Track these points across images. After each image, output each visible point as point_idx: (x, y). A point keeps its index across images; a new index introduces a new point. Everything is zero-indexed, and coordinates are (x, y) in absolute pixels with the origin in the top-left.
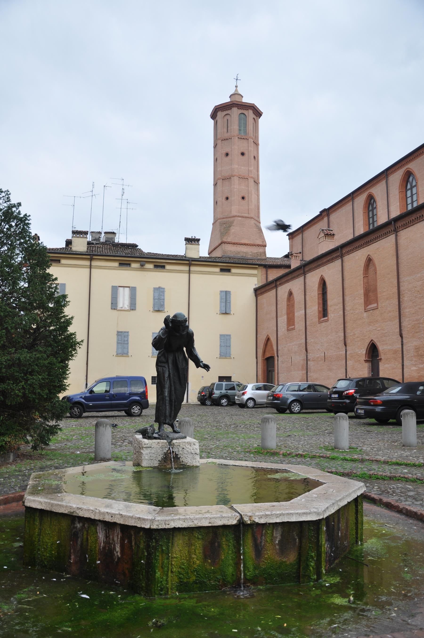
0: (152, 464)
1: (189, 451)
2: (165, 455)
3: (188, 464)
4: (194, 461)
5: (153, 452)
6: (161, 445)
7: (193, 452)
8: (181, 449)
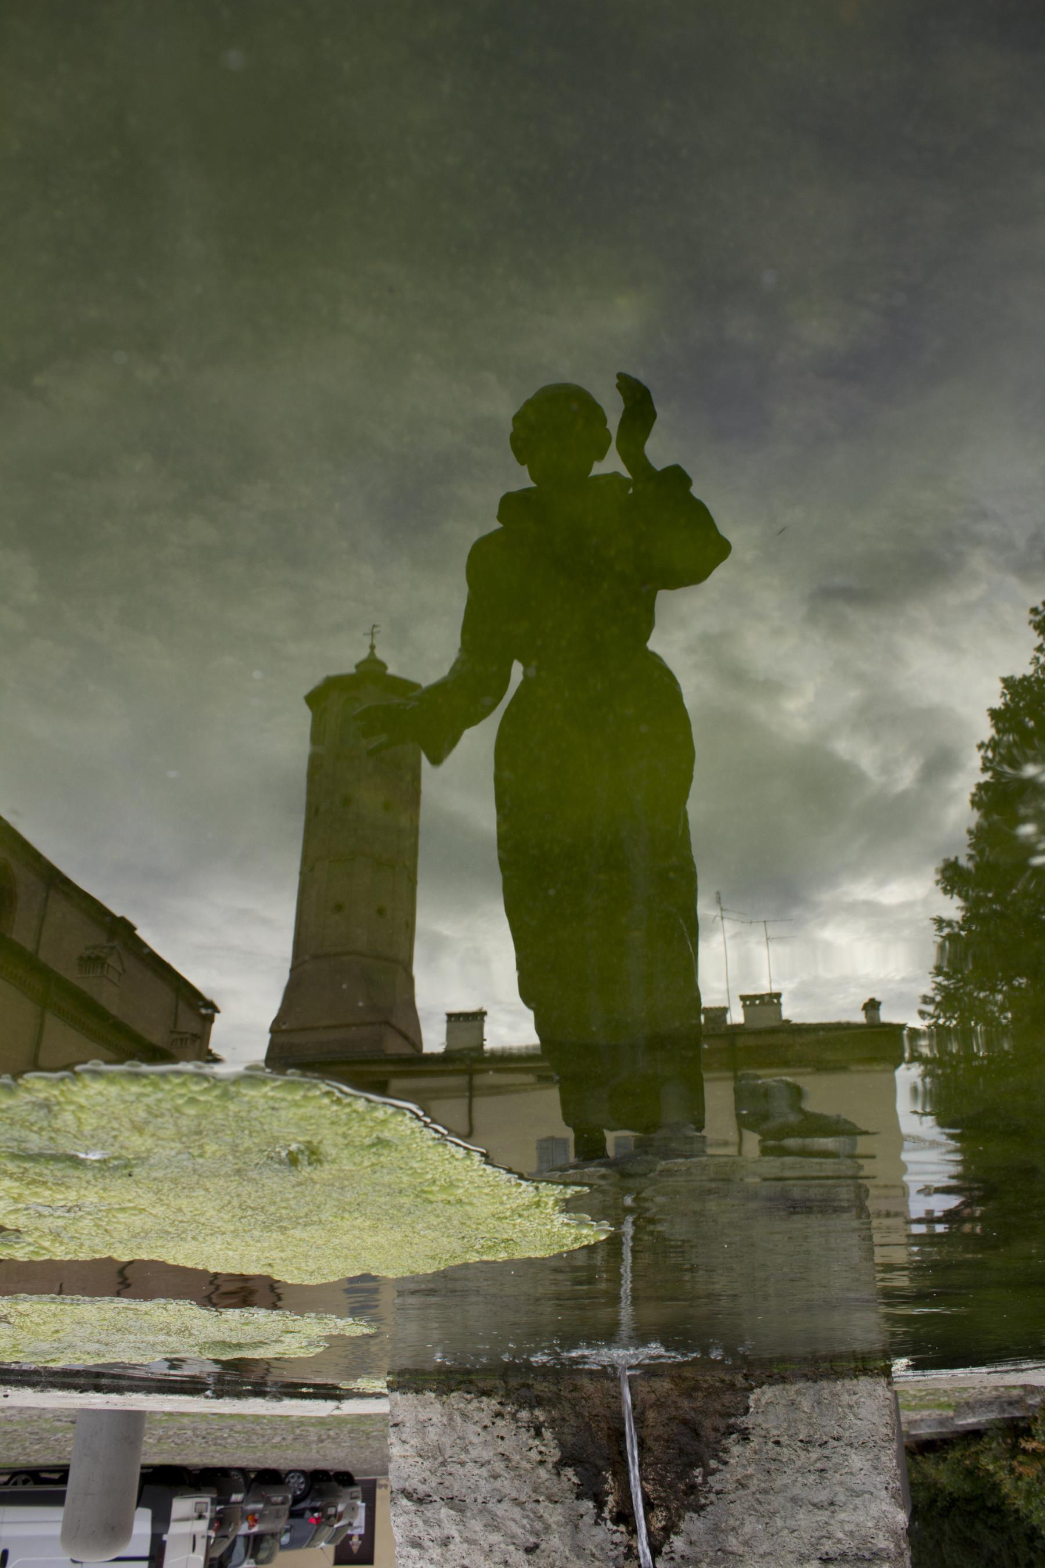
0: (806, 1404)
1: (476, 1525)
2: (692, 1488)
3: (491, 1404)
4: (432, 1435)
5: (804, 1519)
7: (445, 1512)
8: (556, 1542)
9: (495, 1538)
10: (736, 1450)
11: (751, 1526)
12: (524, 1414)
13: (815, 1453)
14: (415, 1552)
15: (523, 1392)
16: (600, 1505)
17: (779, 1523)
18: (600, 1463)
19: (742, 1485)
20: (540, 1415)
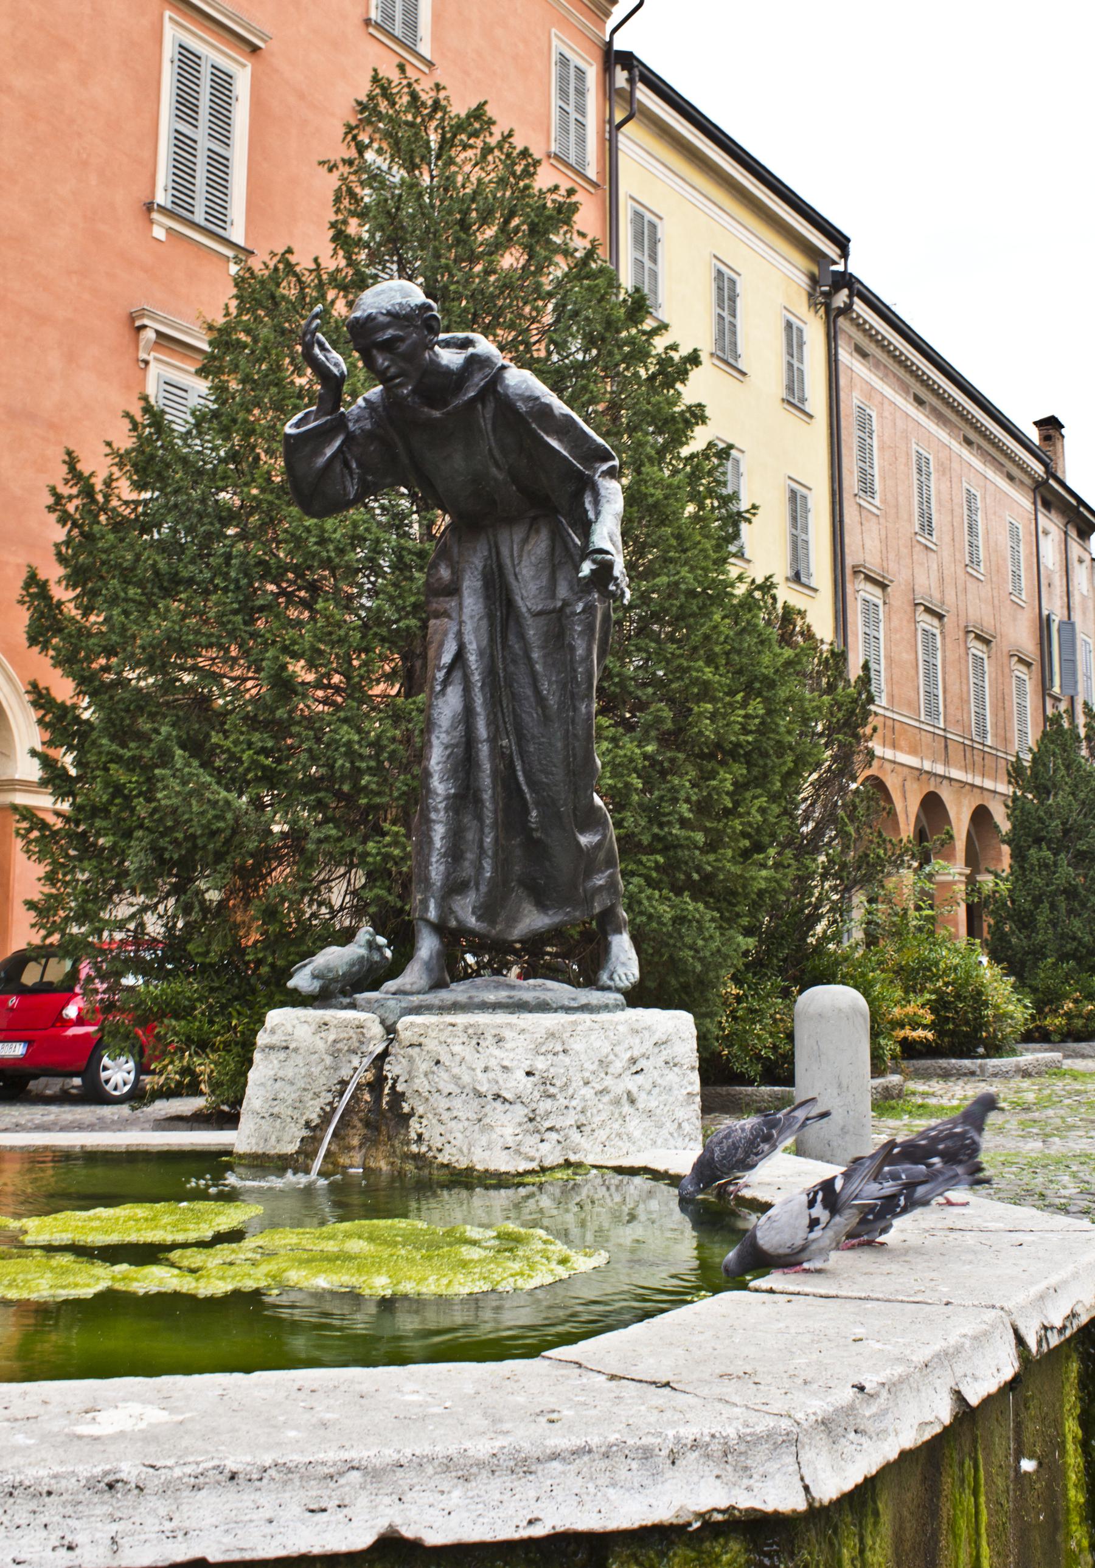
1: (466, 1079)
3: (443, 1158)
4: (484, 1140)
5: (289, 1073)
6: (332, 1038)
7: (483, 1089)
9: (456, 1070)
10: (314, 1116)
11: (316, 1070)
12: (424, 1149)
13: (275, 1111)
14: (506, 1063)
15: (420, 1164)
16: (393, 1087)
17: (303, 1071)
18: (389, 1115)
19: (317, 1095)
20: (414, 1148)
